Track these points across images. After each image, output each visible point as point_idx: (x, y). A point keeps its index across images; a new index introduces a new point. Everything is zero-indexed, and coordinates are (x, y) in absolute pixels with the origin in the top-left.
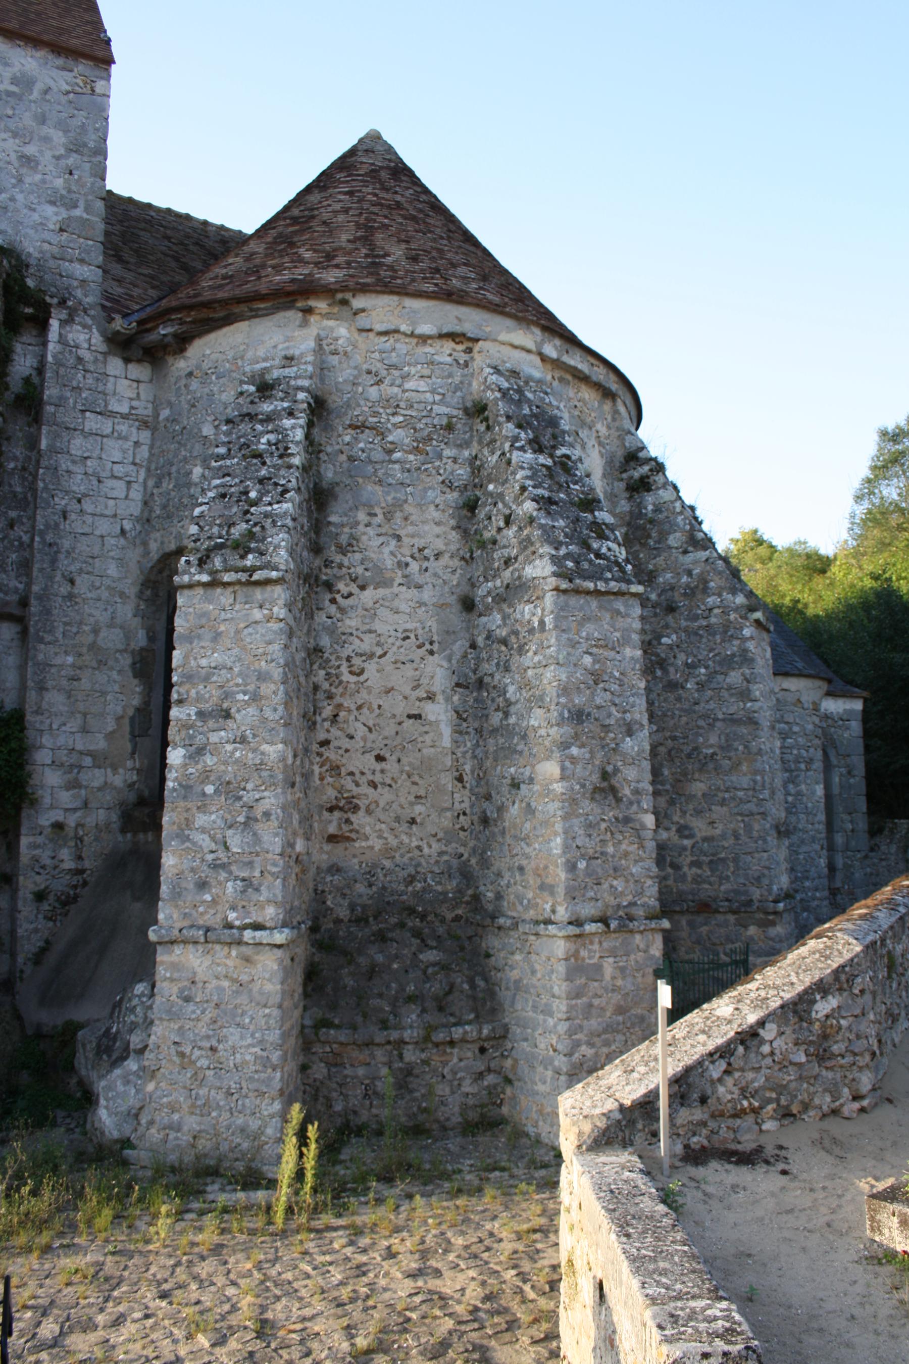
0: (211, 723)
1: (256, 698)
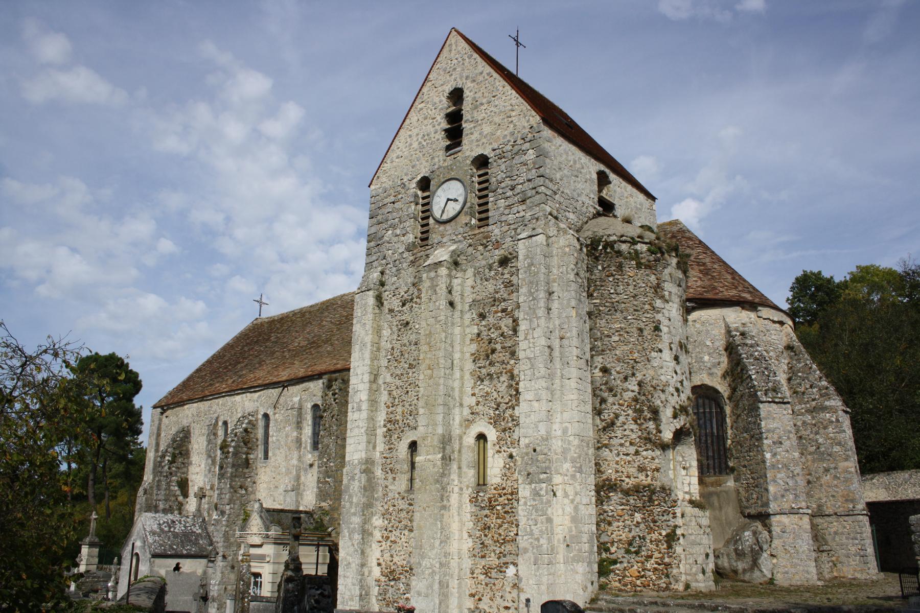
1: (789, 438)
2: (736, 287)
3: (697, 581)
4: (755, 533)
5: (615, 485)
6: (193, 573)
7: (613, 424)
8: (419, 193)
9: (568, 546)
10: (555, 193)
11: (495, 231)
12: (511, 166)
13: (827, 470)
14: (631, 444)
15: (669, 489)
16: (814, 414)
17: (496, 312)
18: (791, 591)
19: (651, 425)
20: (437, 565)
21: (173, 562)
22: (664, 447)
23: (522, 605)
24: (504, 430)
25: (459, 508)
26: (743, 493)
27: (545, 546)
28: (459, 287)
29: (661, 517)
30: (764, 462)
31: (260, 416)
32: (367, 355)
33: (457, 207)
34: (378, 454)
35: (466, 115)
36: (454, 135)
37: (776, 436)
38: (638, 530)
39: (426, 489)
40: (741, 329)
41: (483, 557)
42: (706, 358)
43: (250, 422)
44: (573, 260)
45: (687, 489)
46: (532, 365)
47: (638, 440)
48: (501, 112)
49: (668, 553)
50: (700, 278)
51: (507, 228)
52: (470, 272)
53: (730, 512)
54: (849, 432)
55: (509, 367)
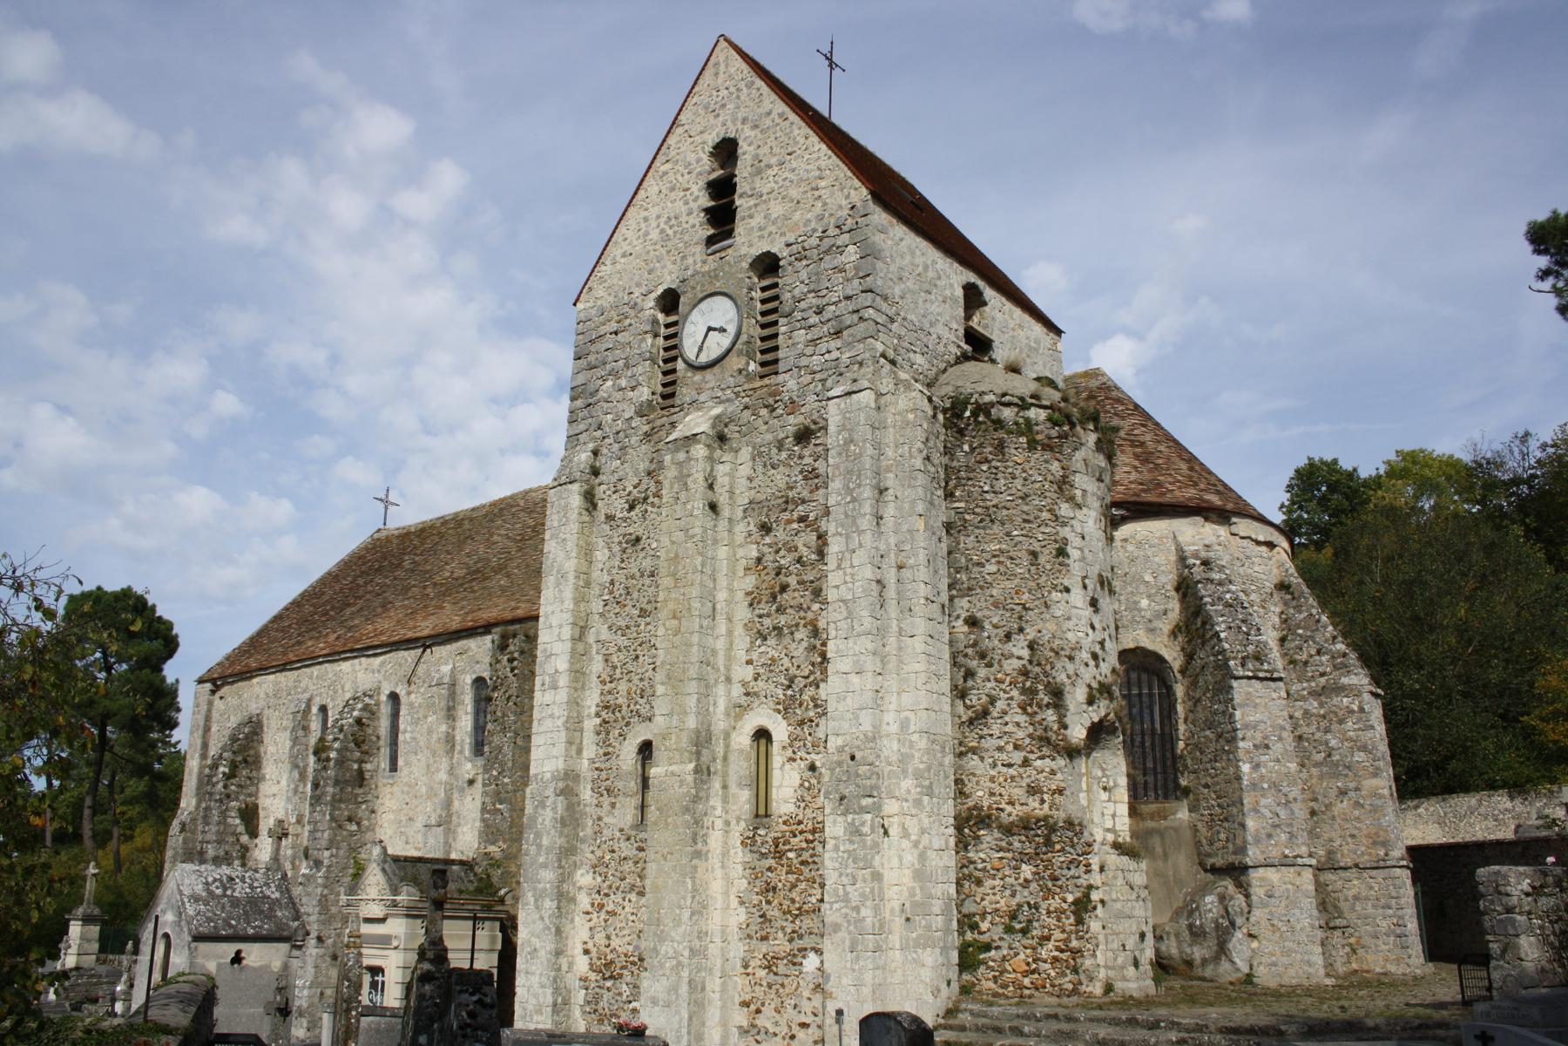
1: (1280, 739)
2: (1195, 484)
3: (1125, 979)
5: (989, 817)
6: (266, 968)
7: (985, 713)
8: (661, 317)
9: (908, 919)
10: (892, 321)
11: (789, 383)
12: (817, 274)
13: (1343, 793)
14: (1016, 747)
15: (1080, 824)
16: (1323, 698)
17: (789, 522)
18: (1282, 995)
19: (1050, 716)
20: (686, 953)
21: (230, 949)
22: (1072, 753)
23: (830, 1020)
24: (801, 723)
25: (723, 855)
27: (869, 920)
28: (727, 479)
29: (1065, 872)
30: (1239, 778)
31: (383, 698)
32: (568, 593)
33: (725, 341)
34: (586, 762)
35: (742, 185)
36: (722, 217)
37: (1259, 736)
38: (1026, 893)
39: (667, 824)
40: (1203, 554)
41: (764, 938)
42: (1144, 603)
43: (366, 708)
44: (920, 435)
45: (1109, 825)
46: (850, 613)
47: (1028, 741)
48: (802, 180)
49: (1077, 932)
50: (1135, 467)
51: (809, 378)
52: (745, 453)
53: (1182, 862)
54: (1381, 729)
55: (810, 615)
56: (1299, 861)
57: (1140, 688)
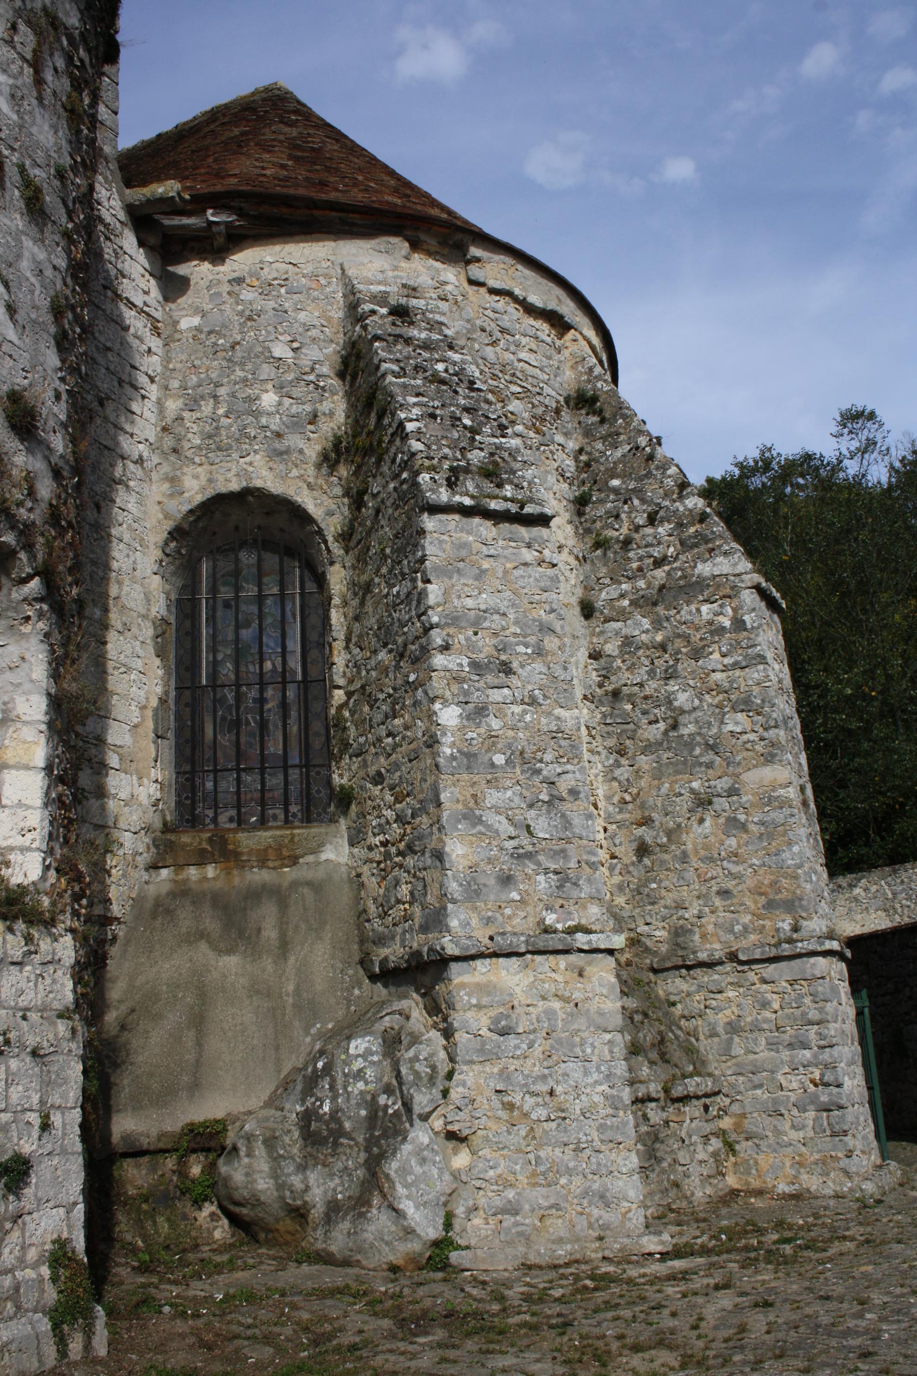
0: (490, 679)
1: (540, 652)
4: (392, 1043)
13: (703, 802)
16: (661, 610)
26: (371, 882)
30: (432, 742)
37: (485, 645)
42: (269, 399)
53: (322, 962)
54: (778, 671)
56: (581, 939)
57: (260, 585)
